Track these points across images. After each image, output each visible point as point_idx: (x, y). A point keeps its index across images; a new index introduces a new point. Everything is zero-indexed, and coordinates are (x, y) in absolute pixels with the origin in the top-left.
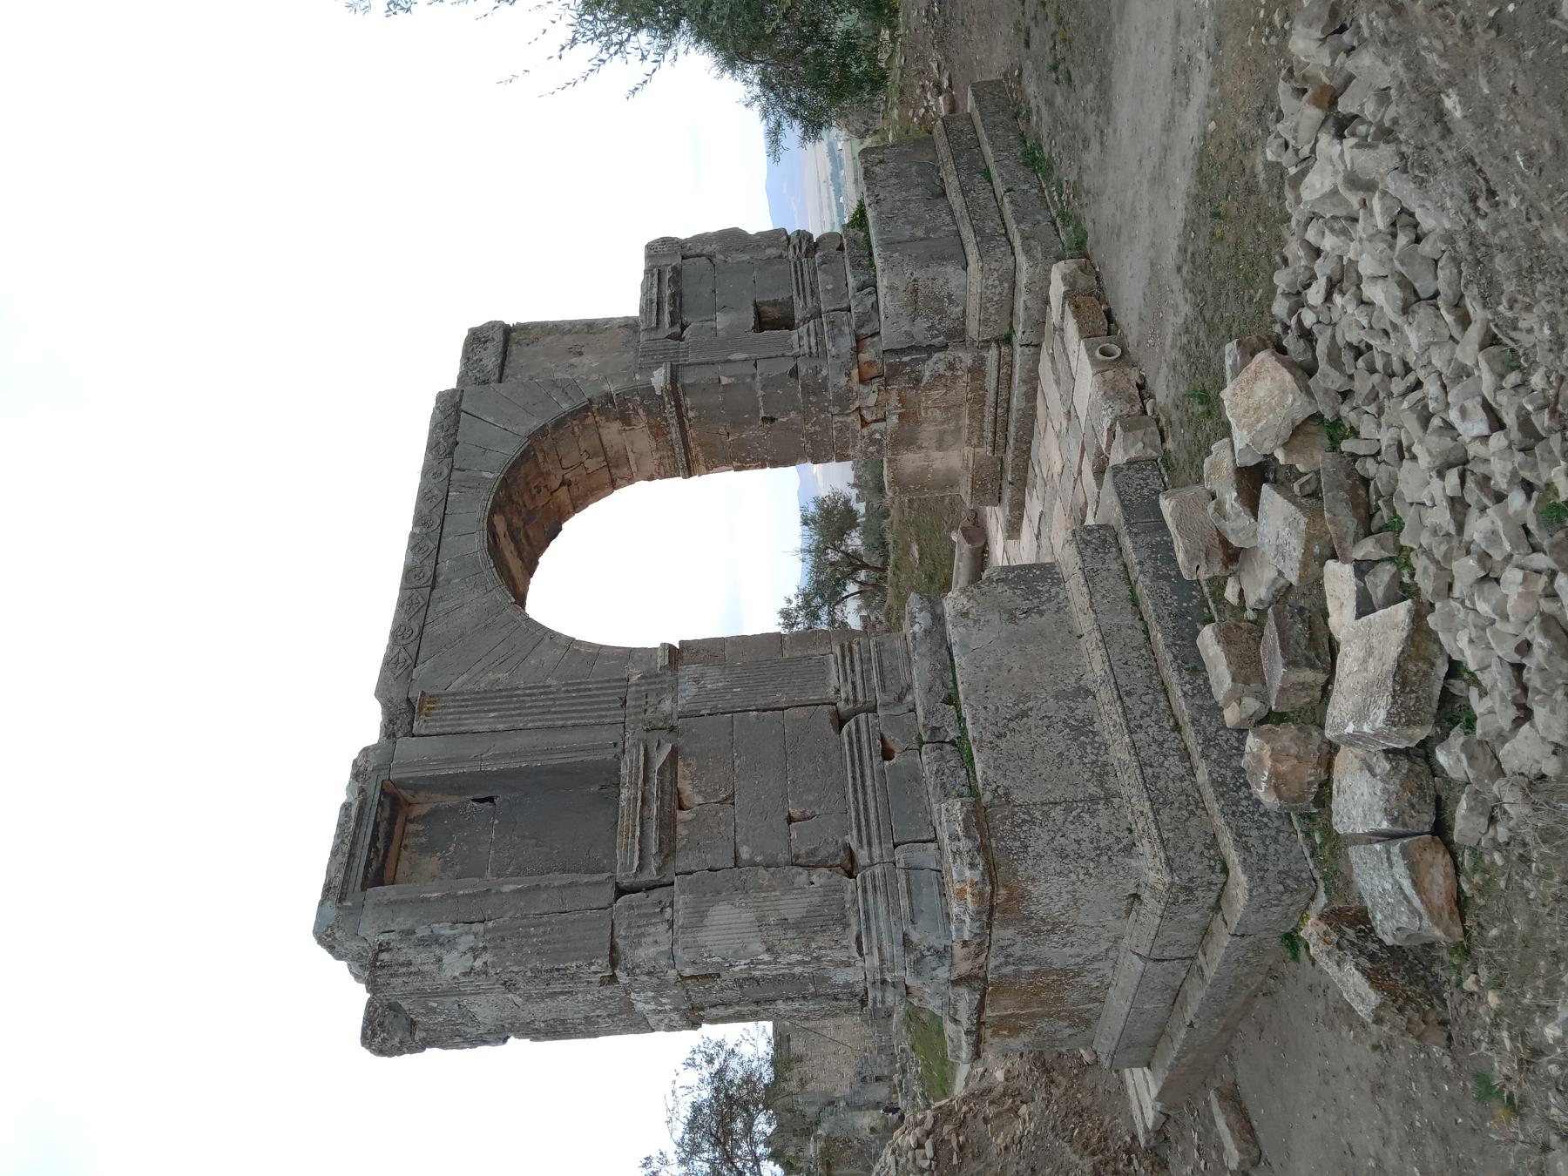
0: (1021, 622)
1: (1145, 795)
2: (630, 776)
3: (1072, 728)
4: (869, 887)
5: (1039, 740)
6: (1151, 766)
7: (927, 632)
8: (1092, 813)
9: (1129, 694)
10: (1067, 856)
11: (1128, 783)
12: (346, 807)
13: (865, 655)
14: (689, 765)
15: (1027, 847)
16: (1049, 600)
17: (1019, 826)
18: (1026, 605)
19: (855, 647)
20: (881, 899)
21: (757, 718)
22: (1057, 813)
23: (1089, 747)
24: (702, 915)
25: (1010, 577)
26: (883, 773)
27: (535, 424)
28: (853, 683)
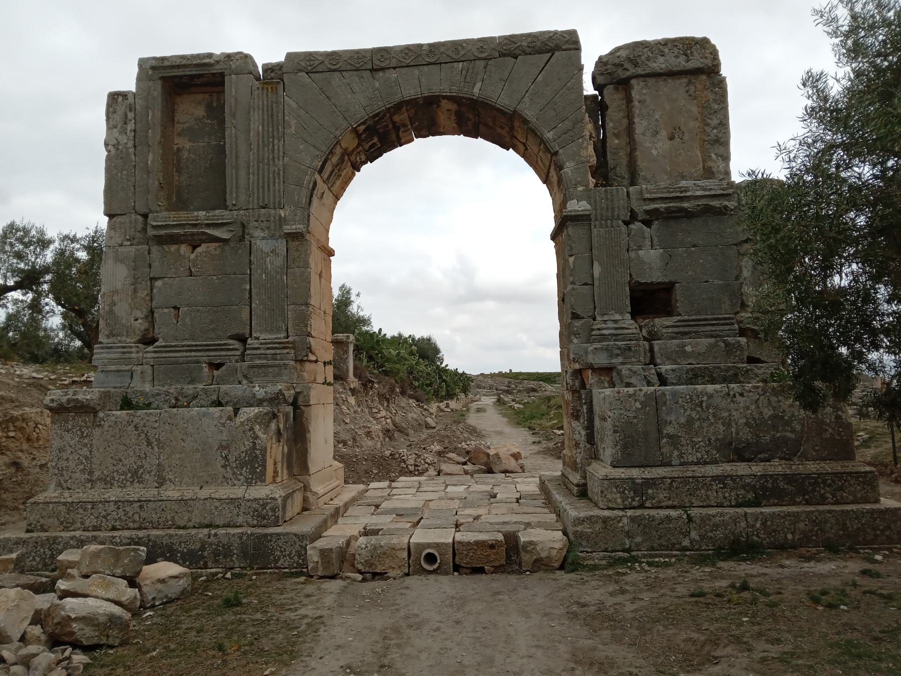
0: (218, 452)
1: (75, 501)
2: (213, 216)
3: (136, 472)
4: (125, 350)
5: (131, 450)
6: (92, 508)
7: (254, 395)
8: (83, 471)
9: (141, 507)
10: (60, 452)
11: (94, 494)
12: (210, 55)
13: (278, 357)
14: (216, 250)
15: (68, 431)
16: (234, 474)
17: (80, 429)
18: (232, 458)
19: (286, 351)
20: (117, 356)
21: (245, 289)
22: (85, 452)
23: (124, 477)
24: (122, 261)
25: (258, 452)
26: (198, 362)
27: (530, 113)
28: (258, 348)
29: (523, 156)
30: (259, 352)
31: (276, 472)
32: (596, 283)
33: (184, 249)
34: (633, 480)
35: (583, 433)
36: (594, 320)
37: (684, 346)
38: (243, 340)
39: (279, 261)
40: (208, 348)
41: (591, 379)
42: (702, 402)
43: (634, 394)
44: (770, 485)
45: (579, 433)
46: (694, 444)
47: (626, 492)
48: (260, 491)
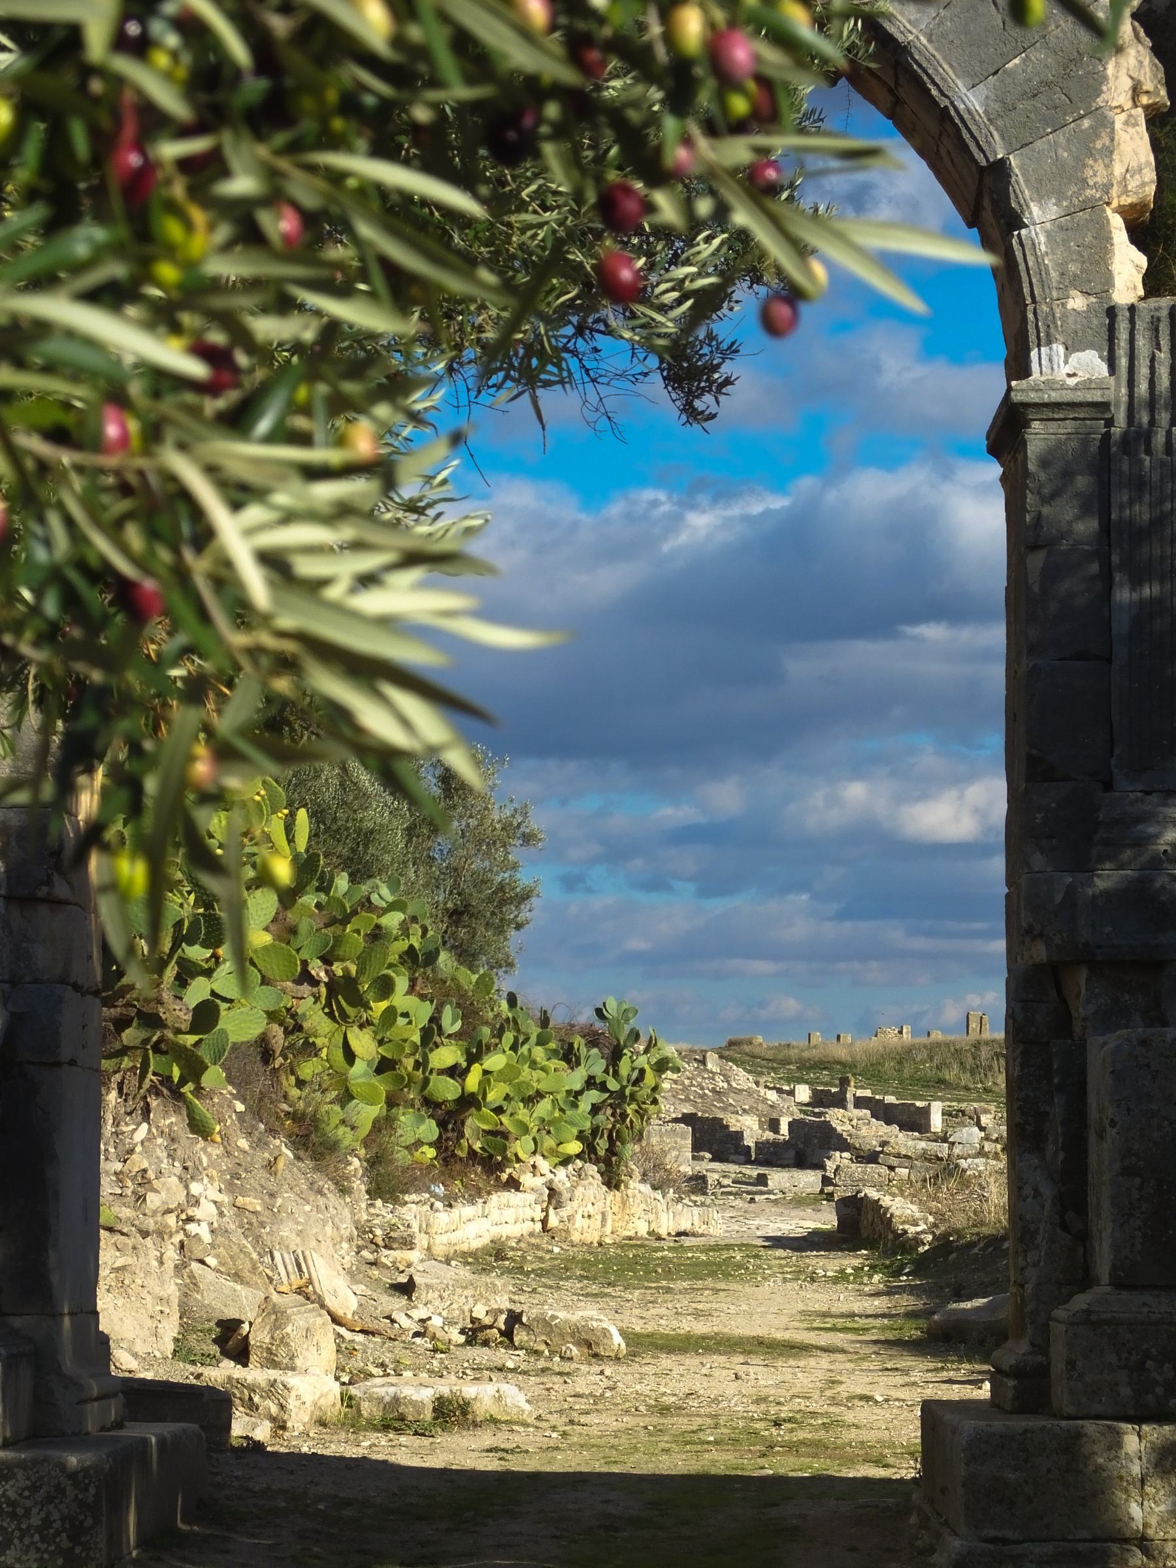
29: (890, 115)
35: (1048, 1191)
45: (1037, 1194)
47: (1150, 1364)
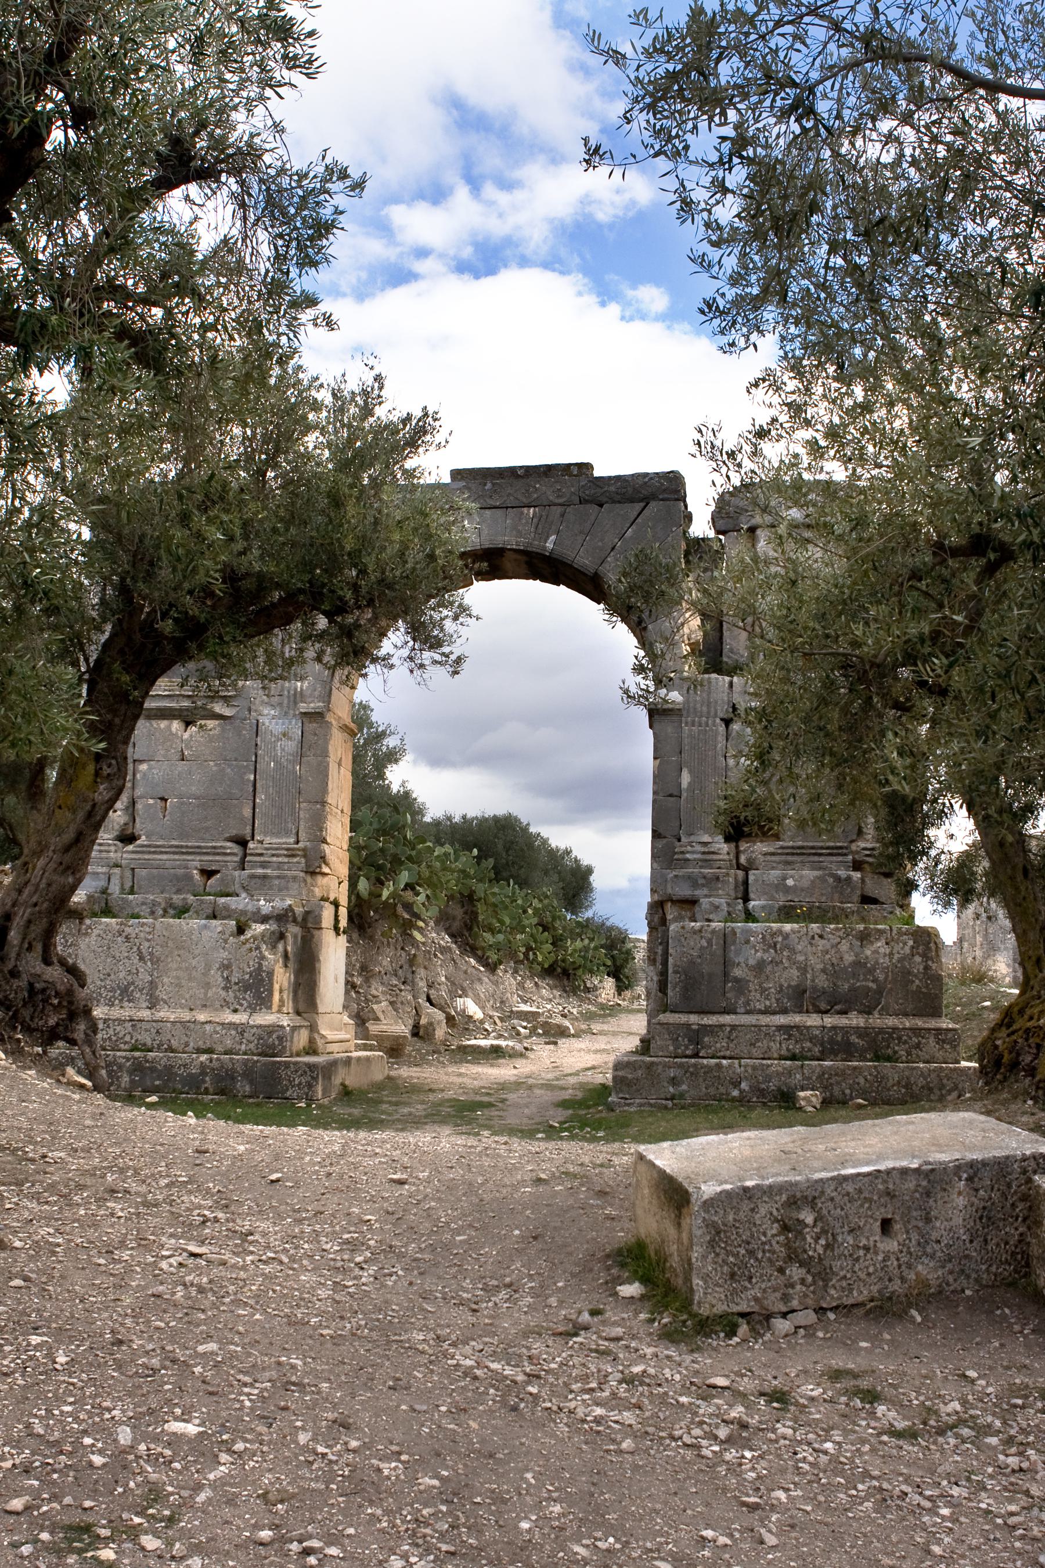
7: (259, 909)
16: (235, 997)
19: (295, 860)
28: (261, 855)
30: (262, 859)
31: (281, 1000)
32: (684, 795)
33: (176, 725)
34: (688, 1026)
36: (679, 840)
37: (785, 879)
38: (242, 843)
39: (291, 746)
40: (197, 851)
41: (671, 912)
42: (775, 944)
43: (700, 931)
44: (839, 1038)
46: (763, 990)
48: (264, 1019)
